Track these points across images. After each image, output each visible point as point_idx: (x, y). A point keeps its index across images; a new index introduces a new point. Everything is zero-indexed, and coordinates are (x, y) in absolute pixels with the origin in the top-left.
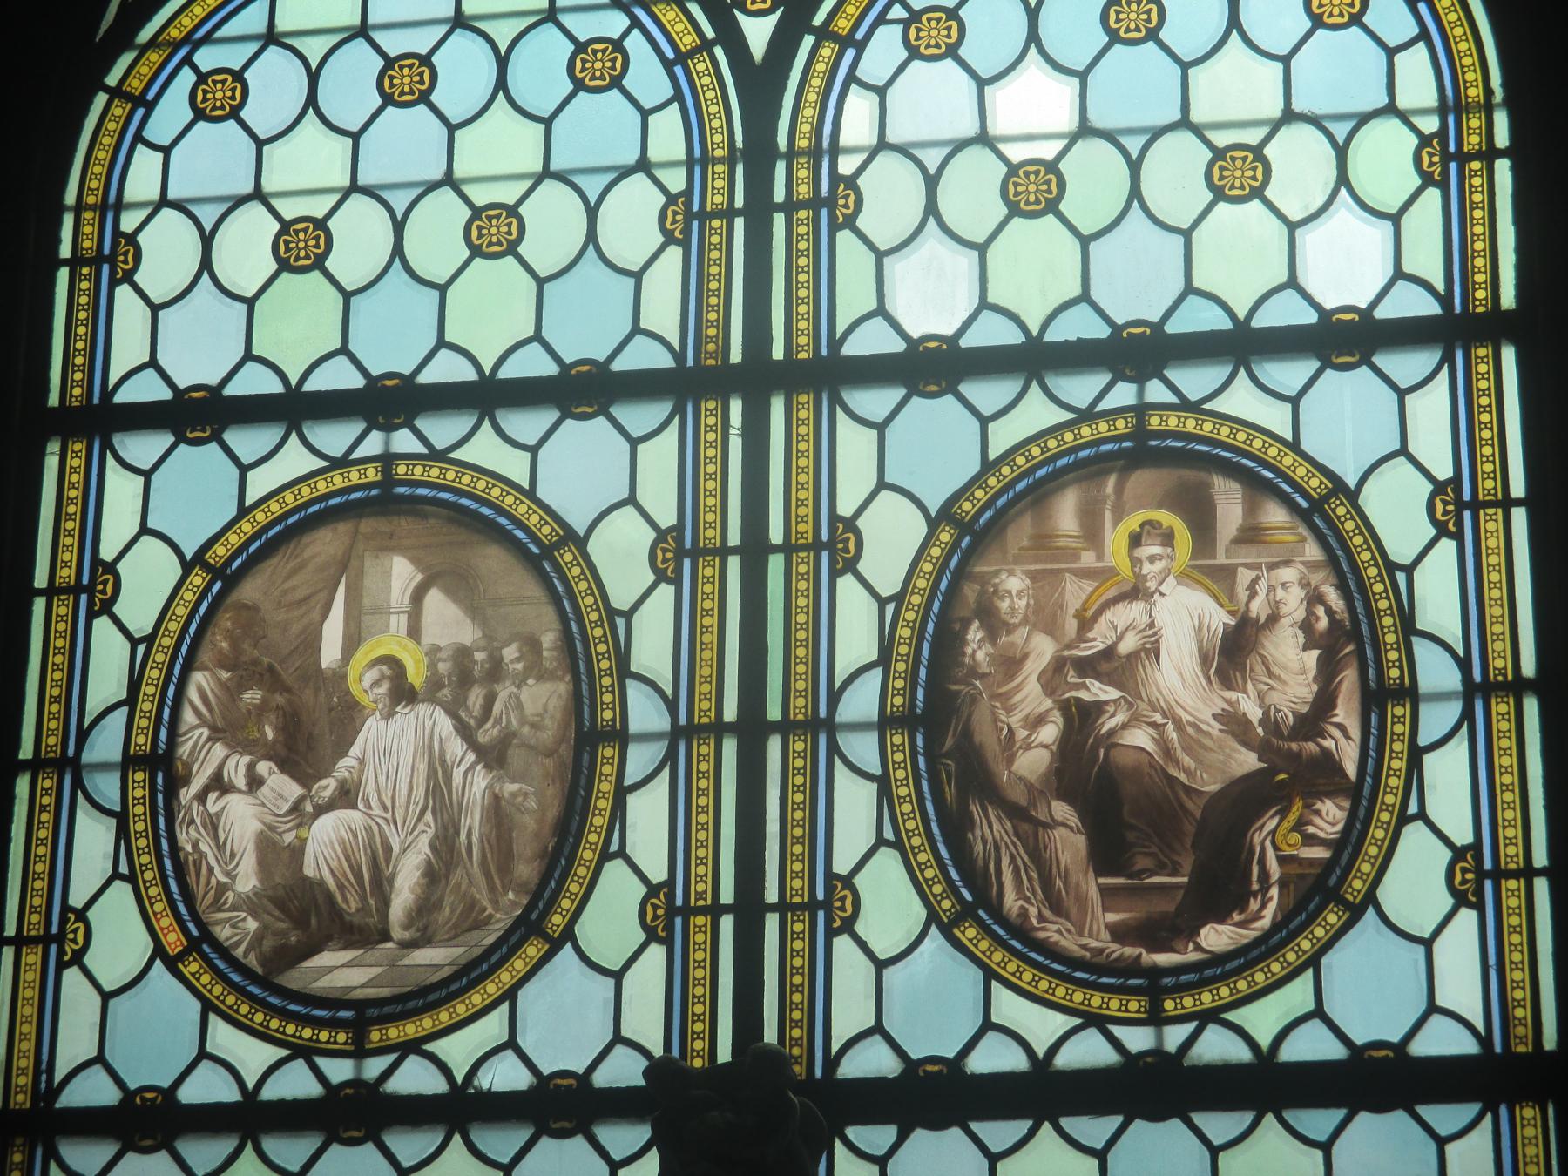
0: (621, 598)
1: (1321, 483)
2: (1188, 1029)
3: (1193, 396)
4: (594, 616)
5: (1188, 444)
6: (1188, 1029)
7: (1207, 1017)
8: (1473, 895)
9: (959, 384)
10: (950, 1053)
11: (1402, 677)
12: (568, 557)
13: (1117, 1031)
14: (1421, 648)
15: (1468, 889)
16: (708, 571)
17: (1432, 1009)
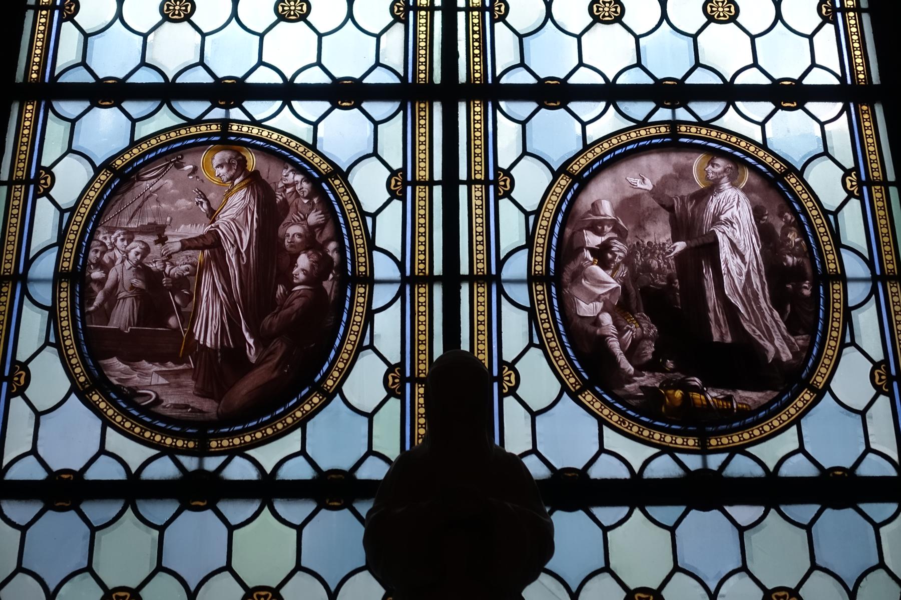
0: (369, 206)
1: (781, 166)
2: (723, 457)
3: (258, 117)
4: (353, 215)
5: (651, 142)
6: (723, 457)
7: (733, 451)
8: (886, 388)
9: (243, 102)
10: (580, 466)
11: (366, 271)
12: (337, 182)
13: (681, 457)
14: (846, 255)
15: (882, 385)
16: (422, 192)
17: (868, 450)
